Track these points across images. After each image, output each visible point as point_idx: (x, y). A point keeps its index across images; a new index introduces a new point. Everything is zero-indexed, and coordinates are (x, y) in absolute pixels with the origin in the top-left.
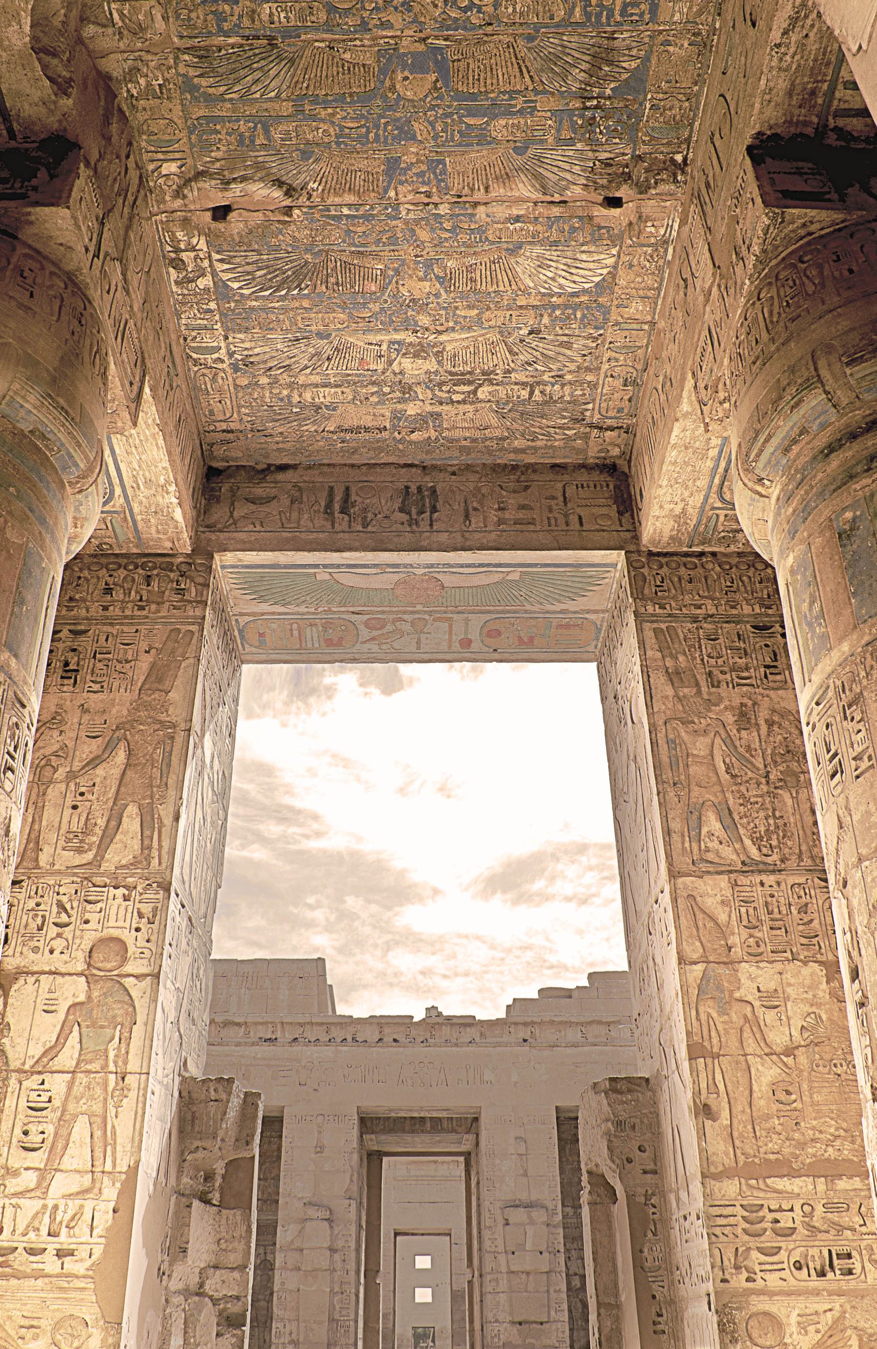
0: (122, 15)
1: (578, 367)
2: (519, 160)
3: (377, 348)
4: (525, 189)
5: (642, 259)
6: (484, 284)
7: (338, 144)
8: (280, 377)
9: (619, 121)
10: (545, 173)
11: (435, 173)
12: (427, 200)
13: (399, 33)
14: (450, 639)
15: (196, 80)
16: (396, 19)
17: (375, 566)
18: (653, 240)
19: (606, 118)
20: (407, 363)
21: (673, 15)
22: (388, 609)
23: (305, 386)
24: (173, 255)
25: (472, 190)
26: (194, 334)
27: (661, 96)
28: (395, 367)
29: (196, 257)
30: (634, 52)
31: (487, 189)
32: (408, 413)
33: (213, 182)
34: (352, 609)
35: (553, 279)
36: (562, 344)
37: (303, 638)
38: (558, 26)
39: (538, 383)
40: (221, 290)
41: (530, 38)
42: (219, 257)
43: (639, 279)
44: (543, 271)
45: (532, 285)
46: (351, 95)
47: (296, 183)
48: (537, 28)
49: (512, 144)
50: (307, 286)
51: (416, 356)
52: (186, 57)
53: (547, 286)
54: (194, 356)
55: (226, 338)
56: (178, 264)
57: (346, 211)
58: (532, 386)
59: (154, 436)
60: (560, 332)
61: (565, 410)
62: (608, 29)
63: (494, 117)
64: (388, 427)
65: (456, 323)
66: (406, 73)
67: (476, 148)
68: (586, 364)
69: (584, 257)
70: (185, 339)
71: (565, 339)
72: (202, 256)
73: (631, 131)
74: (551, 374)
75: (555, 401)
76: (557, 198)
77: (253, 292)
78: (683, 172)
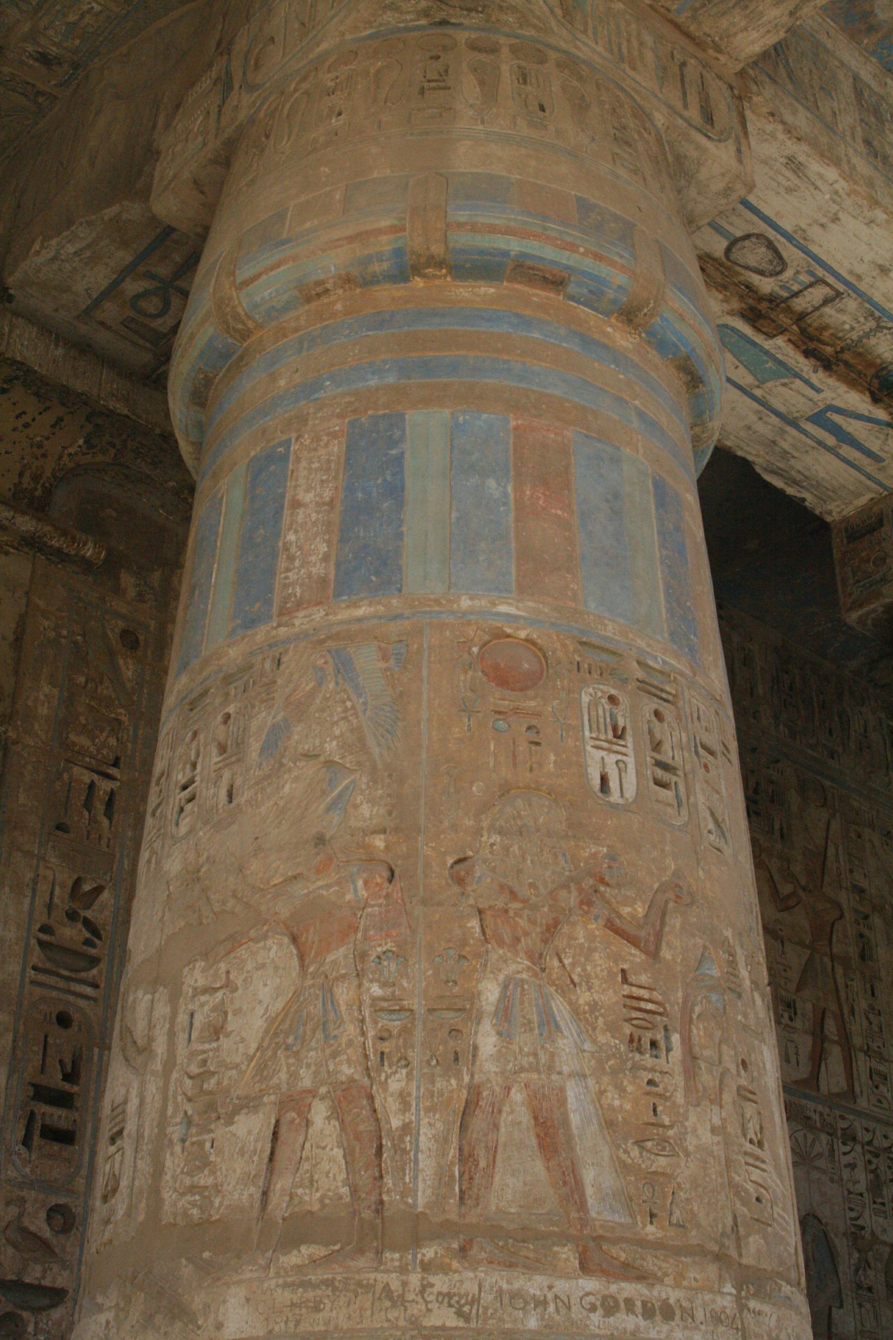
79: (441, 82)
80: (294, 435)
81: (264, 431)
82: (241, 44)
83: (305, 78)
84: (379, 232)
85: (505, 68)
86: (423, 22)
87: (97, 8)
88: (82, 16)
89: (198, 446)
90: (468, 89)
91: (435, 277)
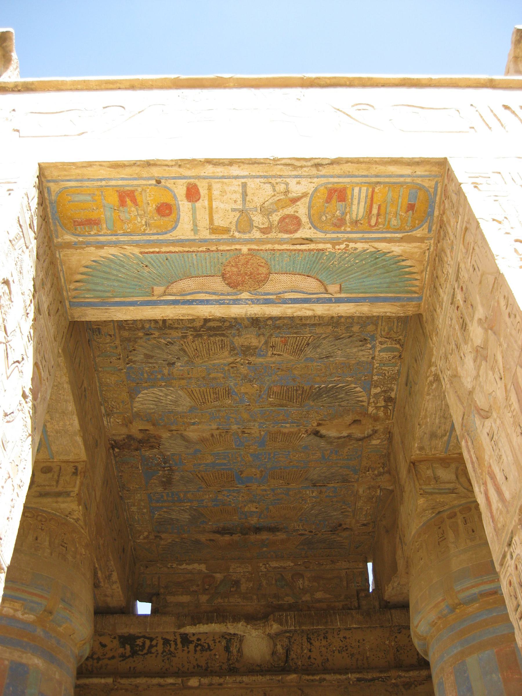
0: (376, 492)
1: (136, 342)
2: (198, 447)
3: (275, 352)
6: (208, 391)
10: (183, 442)
13: (259, 488)
14: (210, 200)
17: (285, 302)
18: (115, 415)
19: (158, 464)
20: (254, 342)
22: (277, 247)
24: (389, 404)
25: (220, 435)
26: (393, 361)
27: (136, 472)
28: (263, 340)
30: (153, 485)
31: (212, 435)
33: (356, 436)
34: (312, 246)
36: (152, 357)
37: (369, 200)
38: (190, 491)
39: (161, 329)
40: (368, 385)
41: (201, 488)
42: (364, 403)
43: (116, 396)
44: (173, 399)
45: (179, 392)
46: (281, 469)
47: (312, 436)
50: (315, 389)
51: (248, 348)
52: (353, 480)
54: (398, 346)
55: (373, 358)
56: (388, 400)
57: (288, 425)
59: (425, 417)
60: (155, 365)
66: (255, 477)
67: (220, 452)
68: (131, 344)
69: (152, 406)
71: (150, 361)
72: (373, 404)
74: (154, 336)
77: (347, 385)
78: (112, 444)
87: (369, 507)
88: (366, 511)
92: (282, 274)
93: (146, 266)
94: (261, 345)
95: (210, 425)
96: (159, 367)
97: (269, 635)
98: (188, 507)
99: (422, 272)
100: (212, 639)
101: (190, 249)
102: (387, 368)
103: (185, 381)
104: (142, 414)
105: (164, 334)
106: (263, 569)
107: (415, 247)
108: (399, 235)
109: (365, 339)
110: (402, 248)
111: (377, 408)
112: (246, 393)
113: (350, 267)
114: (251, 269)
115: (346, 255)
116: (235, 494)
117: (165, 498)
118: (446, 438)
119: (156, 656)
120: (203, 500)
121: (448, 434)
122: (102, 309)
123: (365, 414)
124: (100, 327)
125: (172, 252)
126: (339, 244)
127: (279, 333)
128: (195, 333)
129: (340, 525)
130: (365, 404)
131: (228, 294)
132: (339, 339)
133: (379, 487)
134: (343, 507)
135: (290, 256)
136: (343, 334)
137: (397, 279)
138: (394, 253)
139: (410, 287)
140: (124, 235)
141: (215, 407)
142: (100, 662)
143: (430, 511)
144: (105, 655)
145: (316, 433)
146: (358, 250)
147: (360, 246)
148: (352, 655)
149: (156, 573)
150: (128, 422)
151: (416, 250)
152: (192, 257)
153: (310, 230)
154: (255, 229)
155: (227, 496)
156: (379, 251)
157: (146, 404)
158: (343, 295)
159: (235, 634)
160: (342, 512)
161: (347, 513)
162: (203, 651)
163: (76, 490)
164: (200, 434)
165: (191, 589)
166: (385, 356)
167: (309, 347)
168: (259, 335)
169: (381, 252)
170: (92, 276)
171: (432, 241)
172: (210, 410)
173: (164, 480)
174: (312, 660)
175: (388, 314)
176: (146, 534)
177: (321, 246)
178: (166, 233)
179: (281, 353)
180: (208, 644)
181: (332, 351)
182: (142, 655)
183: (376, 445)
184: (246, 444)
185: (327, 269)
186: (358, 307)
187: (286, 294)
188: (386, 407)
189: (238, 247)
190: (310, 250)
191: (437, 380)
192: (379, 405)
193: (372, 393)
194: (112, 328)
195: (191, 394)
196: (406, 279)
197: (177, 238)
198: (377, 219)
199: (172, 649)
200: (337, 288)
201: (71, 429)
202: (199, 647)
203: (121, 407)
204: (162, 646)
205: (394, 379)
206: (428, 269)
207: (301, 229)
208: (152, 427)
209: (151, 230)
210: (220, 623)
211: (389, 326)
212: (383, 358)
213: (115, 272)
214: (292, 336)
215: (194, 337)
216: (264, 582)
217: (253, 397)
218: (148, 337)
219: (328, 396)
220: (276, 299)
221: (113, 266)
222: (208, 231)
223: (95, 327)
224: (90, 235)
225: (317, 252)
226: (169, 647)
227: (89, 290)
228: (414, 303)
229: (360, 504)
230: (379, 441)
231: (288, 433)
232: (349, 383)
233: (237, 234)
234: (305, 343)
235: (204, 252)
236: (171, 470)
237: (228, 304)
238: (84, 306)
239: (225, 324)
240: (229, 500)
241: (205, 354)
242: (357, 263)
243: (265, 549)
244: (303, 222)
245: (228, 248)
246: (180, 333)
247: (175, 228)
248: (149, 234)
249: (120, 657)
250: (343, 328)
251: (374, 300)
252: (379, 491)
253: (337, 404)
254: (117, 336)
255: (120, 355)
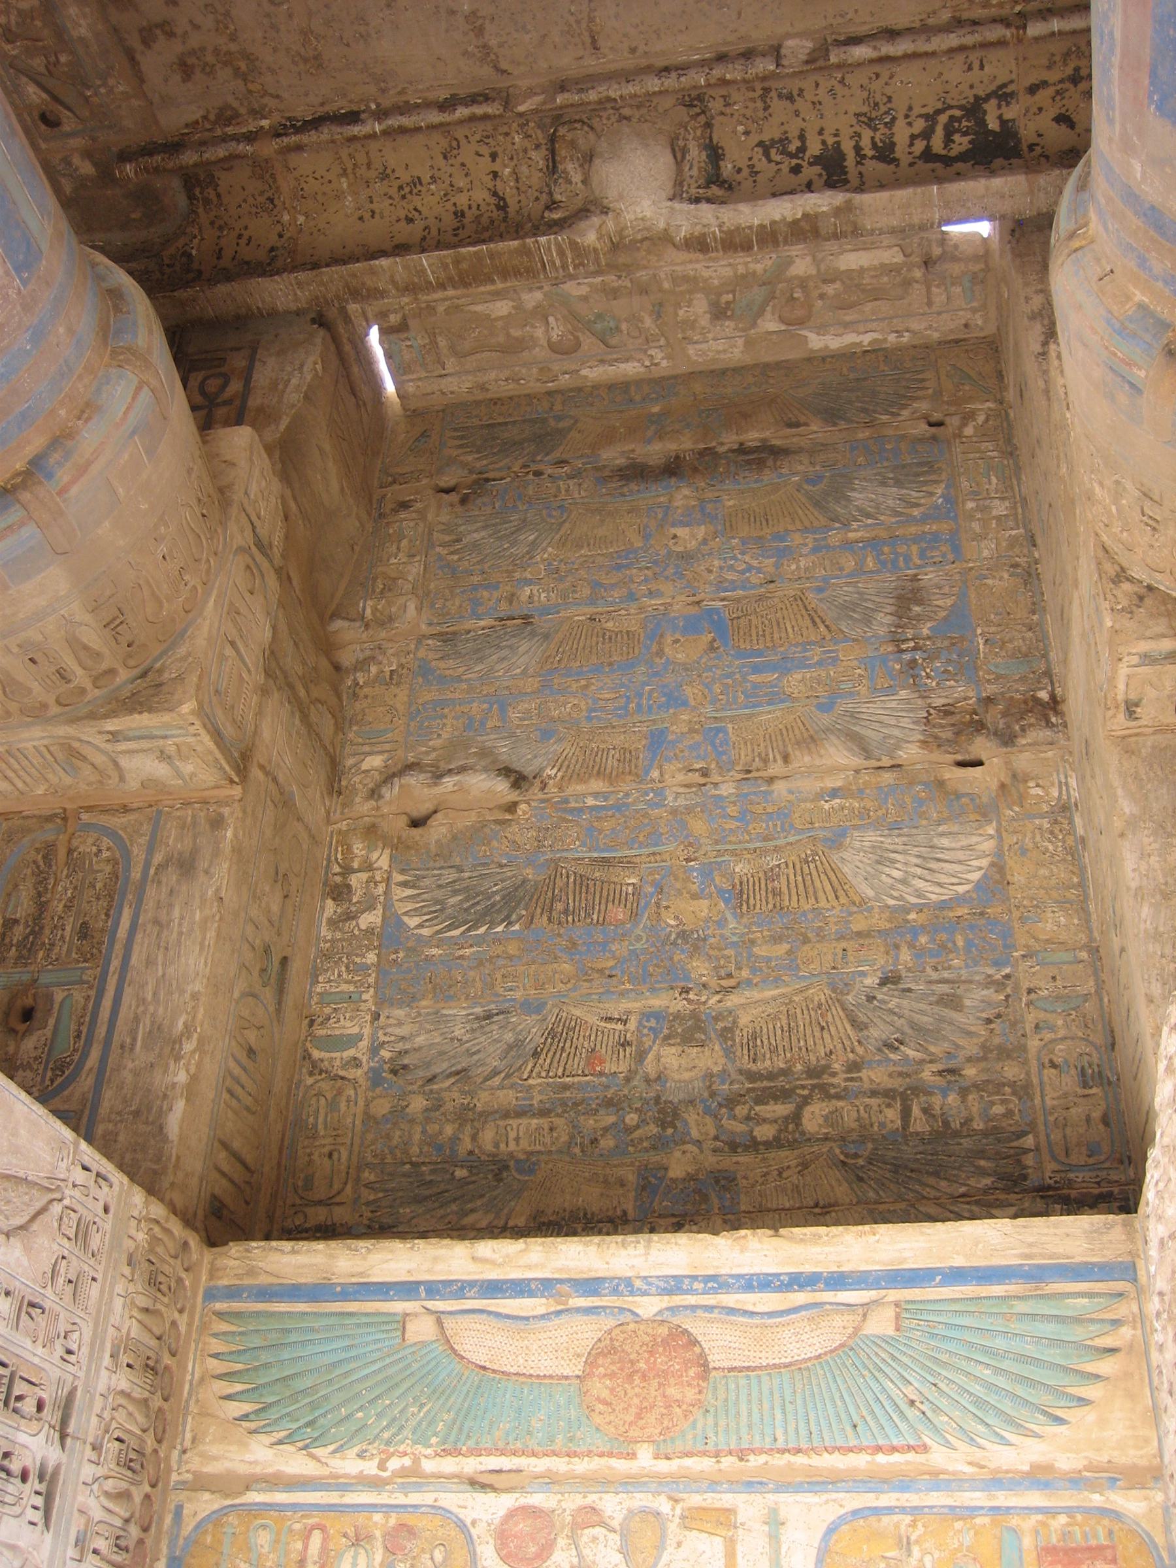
0: (375, 610)
1: (983, 1047)
2: (825, 719)
3: (620, 1027)
4: (839, 754)
5: (1038, 838)
6: (795, 898)
7: (589, 719)
8: (446, 1095)
9: (949, 661)
10: (863, 732)
11: (713, 745)
12: (702, 780)
15: (434, 663)
16: (667, 588)
17: (546, 1286)
18: (1045, 808)
19: (931, 657)
21: (980, 552)
22: (559, 1465)
23: (485, 1115)
24: (338, 879)
25: (765, 761)
26: (327, 1010)
27: (993, 629)
28: (650, 1066)
29: (371, 880)
31: (786, 759)
32: (672, 1174)
33: (422, 777)
34: (470, 1465)
35: (904, 882)
38: (848, 576)
40: (390, 934)
41: (820, 590)
43: (1043, 872)
45: (870, 893)
46: (610, 664)
47: (528, 770)
48: (825, 580)
49: (815, 702)
51: (687, 1039)
52: (430, 642)
53: (895, 894)
54: (316, 1054)
55: (376, 1016)
56: (339, 892)
57: (590, 802)
58: (905, 1098)
60: (935, 976)
61: (981, 1154)
62: (909, 572)
63: (786, 671)
64: (631, 1214)
65: (754, 970)
66: (677, 636)
68: (997, 1041)
69: (945, 842)
70: (312, 1023)
71: (945, 988)
72: (378, 878)
73: (967, 668)
74: (935, 1068)
75: (956, 1134)
76: (886, 761)
77: (438, 932)
78: (1057, 713)
79: (114, 625)
80: (24, 291)
81: (47, 283)
82: (272, 581)
83: (208, 572)
84: (74, 481)
85: (79, 672)
86: (158, 665)
87: (393, 561)
89: (94, 265)
90: (92, 637)
91: (13, 478)
92: (551, 1377)
93: (912, 1402)
94: (655, 1048)
95: (791, 792)
96: (924, 971)
97: (605, 211)
98: (855, 525)
99: (202, 1380)
100: (759, 178)
101: (792, 1458)
102: (344, 987)
103: (855, 928)
104: (972, 817)
105: (908, 1076)
106: (658, 355)
107: (215, 1458)
108: (254, 1497)
109: (394, 1072)
110: (248, 1457)
111: (368, 867)
112: (695, 896)
113: (378, 1397)
114: (631, 1393)
115: (386, 1435)
116: (730, 576)
117: (914, 549)
118: (158, 858)
119: (910, 108)
120: (815, 550)
121: (152, 871)
122: (1043, 1256)
123: (398, 847)
124: (1080, 1091)
125: (839, 1449)
126: (403, 1473)
127: (607, 1087)
128: (827, 1079)
129: (464, 501)
130: (398, 877)
131: (694, 1308)
132: (458, 1073)
133: (367, 626)
134: (456, 557)
135: (529, 1433)
136: (449, 1089)
137: (265, 1357)
138: (266, 1439)
139: (233, 1333)
140: (972, 1511)
141: (777, 849)
142: (1069, 71)
143: (166, 675)
144: (1058, 93)
145: (519, 780)
146: (356, 1450)
147: (350, 1465)
148: (384, 176)
149: (939, 313)
150: (1013, 786)
151: (214, 1450)
152: (786, 1432)
153: (475, 1515)
154: (615, 1524)
155: (750, 568)
156: (306, 1447)
157: (962, 848)
158: (399, 1306)
159: (697, 200)
160: (457, 541)
161: (448, 538)
162: (781, 140)
163: (1123, 671)
164: (818, 762)
165: (838, 285)
166: (348, 1024)
167: (532, 1045)
168: (659, 1078)
169: (300, 1444)
170: (1066, 1370)
171: (174, 1477)
172: (791, 839)
173: (917, 609)
174: (485, 150)
175: (287, 1245)
176: (969, 431)
177: (449, 1465)
178: (855, 1512)
179: (603, 1024)
180: (770, 161)
181: (478, 1034)
182: (951, 107)
183: (371, 753)
184: (698, 738)
185: (434, 1391)
186: (361, 1270)
187: (542, 1311)
188: (347, 870)
189: (663, 1466)
190: (476, 1452)
191: (174, 1042)
192: (364, 876)
193: (379, 911)
194: (1048, 1088)
195: (840, 886)
196: (242, 1358)
197: (825, 1497)
198: (306, 1548)
199: (867, 134)
200: (410, 1327)
201: (1146, 840)
202: (792, 148)
203: (1029, 835)
204: (895, 139)
205: (326, 956)
206: (187, 1387)
207: (497, 1521)
208: (947, 776)
209: (897, 1526)
210: (738, 228)
211: (336, 1115)
212: (352, 1019)
213: (1001, 1382)
214: (576, 1079)
215: (828, 1066)
216: (648, 322)
217: (678, 885)
218: (952, 1064)
219: (489, 898)
220: (569, 1296)
221: (1007, 1406)
222: (740, 1518)
223: (1094, 1090)
224: (1069, 1511)
225: (459, 1445)
226: (877, 140)
227: (1078, 1320)
228: (225, 1282)
229: (414, 570)
230: (365, 766)
231: (590, 775)
232: (436, 940)
233: (663, 1505)
234: (543, 1056)
235: (753, 1451)
236: (897, 641)
237: (694, 1278)
238: (1094, 1264)
239: (746, 1111)
240: (747, 558)
241: (799, 1016)
242: (361, 1408)
243: (656, 409)
244: (492, 1541)
245: (688, 1462)
246: (865, 1079)
247: (831, 1530)
248: (903, 1510)
249: (1012, 95)
250: (449, 1106)
251: (318, 1292)
252: (368, 611)
253: (467, 875)
254: (1034, 1069)
255: (1027, 1005)
